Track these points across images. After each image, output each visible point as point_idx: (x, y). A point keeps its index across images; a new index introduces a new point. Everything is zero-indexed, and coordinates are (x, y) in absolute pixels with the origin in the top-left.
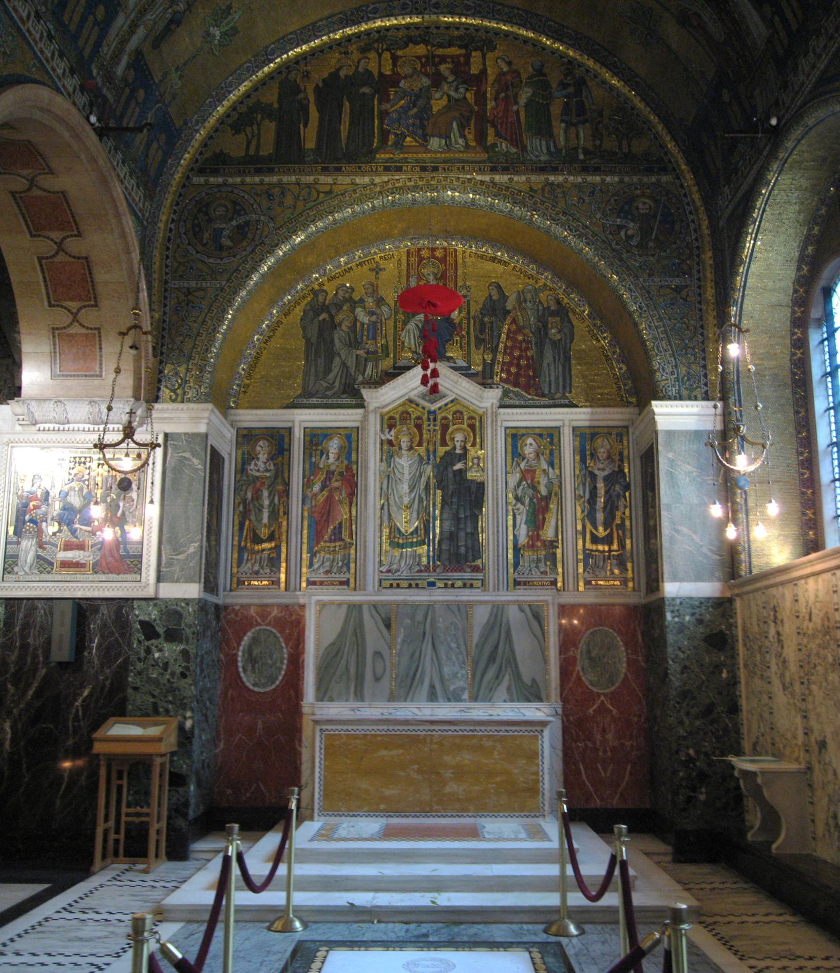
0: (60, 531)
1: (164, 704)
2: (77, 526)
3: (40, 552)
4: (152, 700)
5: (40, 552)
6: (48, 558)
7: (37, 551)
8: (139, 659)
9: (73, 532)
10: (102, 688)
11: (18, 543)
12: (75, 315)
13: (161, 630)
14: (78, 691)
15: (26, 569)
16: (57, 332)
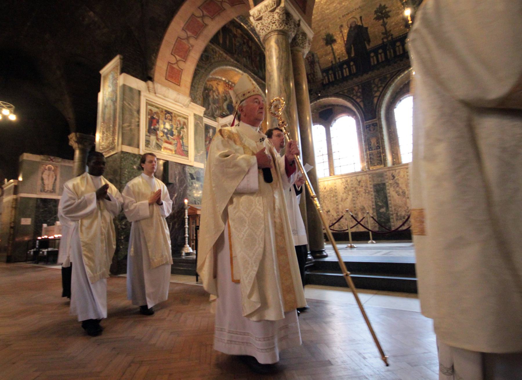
0: (163, 136)
1: (197, 201)
2: (169, 136)
3: (157, 142)
4: (194, 200)
5: (157, 142)
6: (160, 144)
7: (156, 141)
8: (190, 186)
9: (168, 137)
10: (181, 194)
11: (149, 136)
12: (177, 61)
13: (195, 177)
14: (173, 195)
15: (153, 147)
16: (170, 64)
